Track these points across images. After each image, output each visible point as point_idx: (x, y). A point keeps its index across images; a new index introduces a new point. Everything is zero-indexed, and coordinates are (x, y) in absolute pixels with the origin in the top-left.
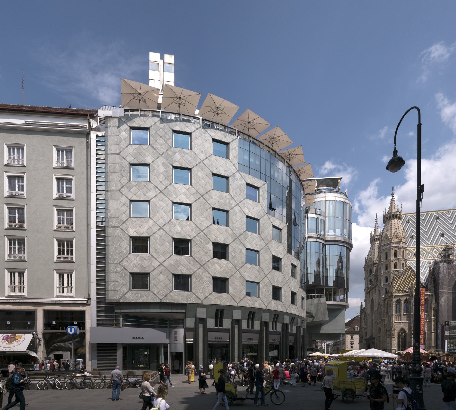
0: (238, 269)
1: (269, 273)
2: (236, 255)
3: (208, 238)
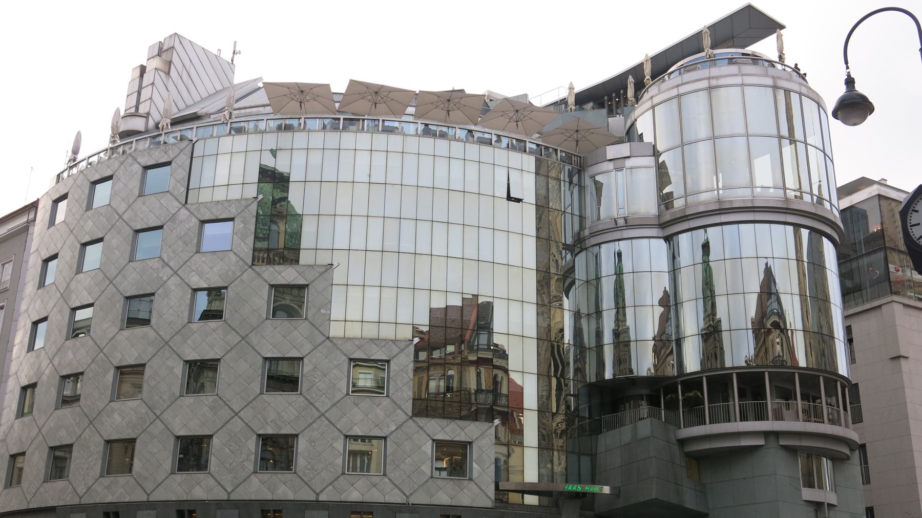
0: (158, 413)
1: (246, 406)
2: (159, 382)
3: (110, 361)
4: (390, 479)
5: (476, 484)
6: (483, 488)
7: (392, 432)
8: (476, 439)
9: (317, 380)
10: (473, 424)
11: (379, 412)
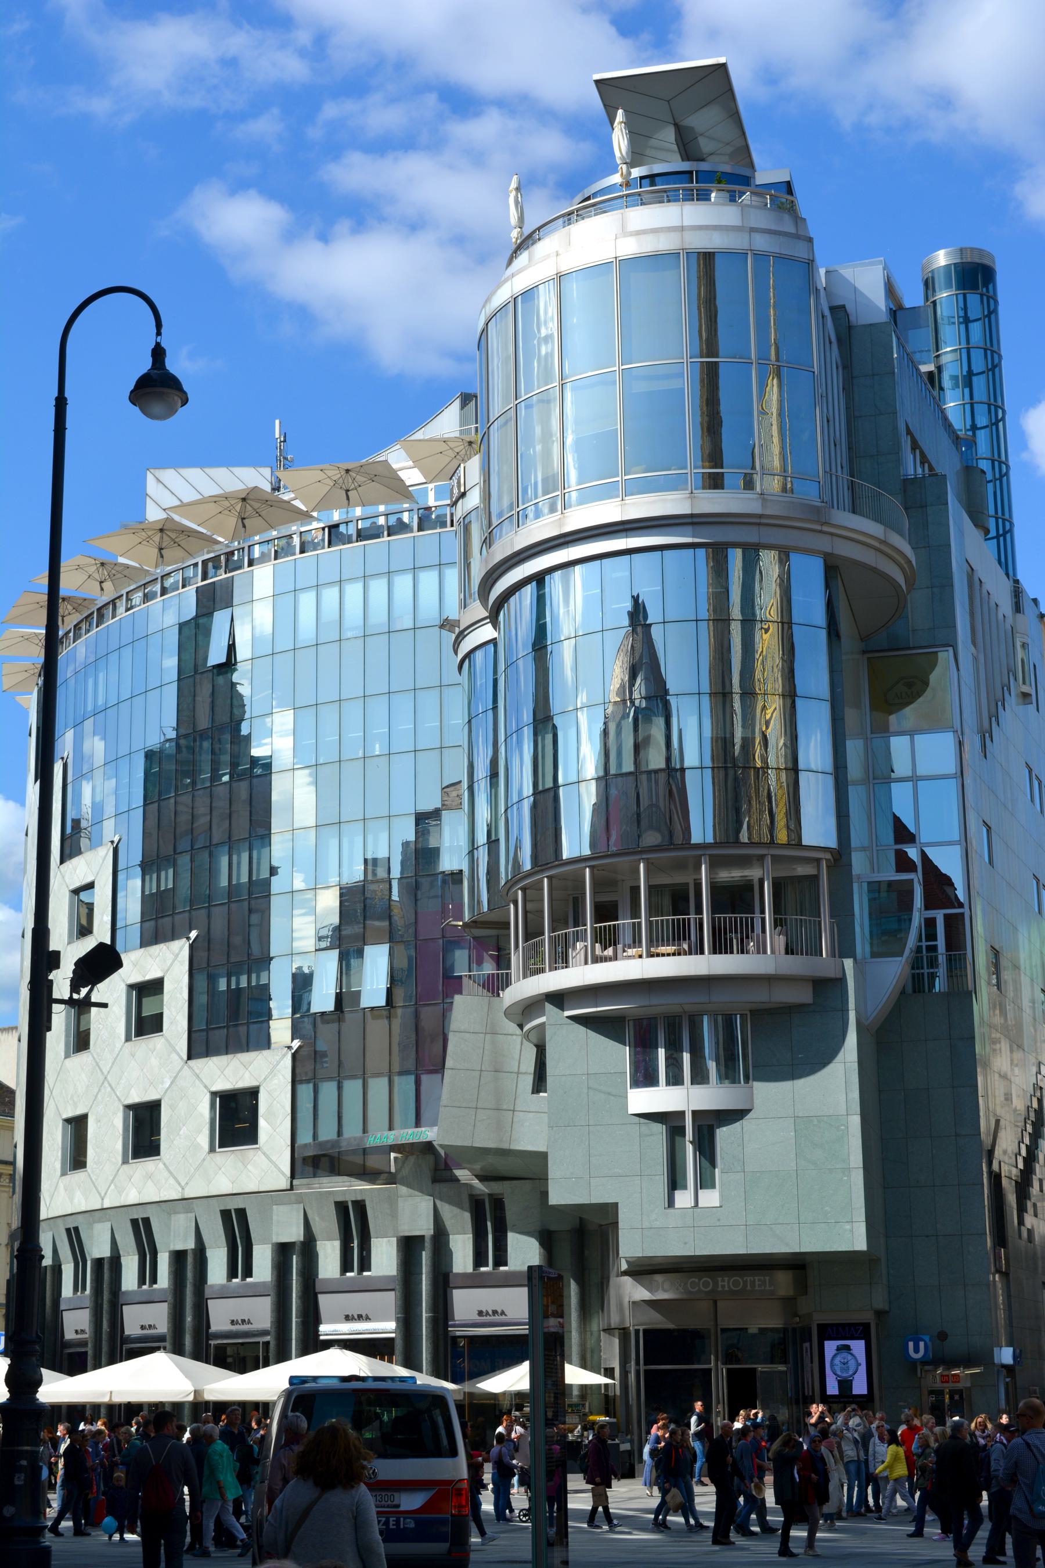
4: (164, 1164)
5: (264, 1154)
6: (274, 1158)
7: (167, 1089)
8: (265, 1079)
9: (101, 1026)
10: (260, 1056)
11: (154, 1061)
